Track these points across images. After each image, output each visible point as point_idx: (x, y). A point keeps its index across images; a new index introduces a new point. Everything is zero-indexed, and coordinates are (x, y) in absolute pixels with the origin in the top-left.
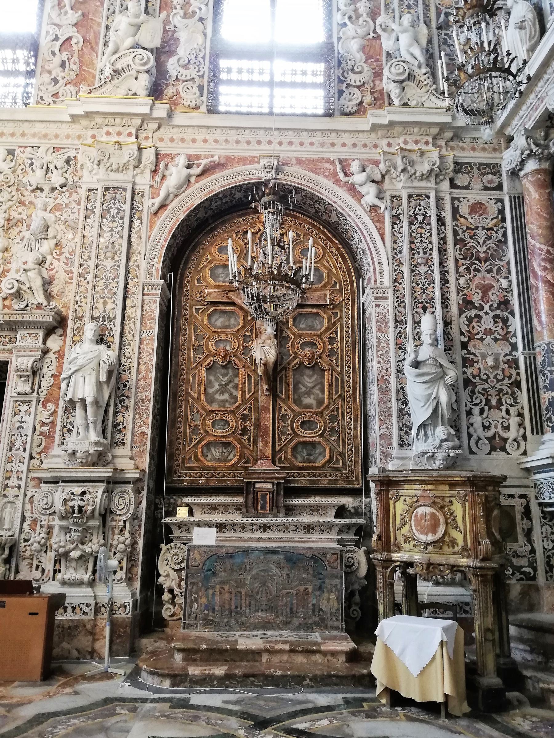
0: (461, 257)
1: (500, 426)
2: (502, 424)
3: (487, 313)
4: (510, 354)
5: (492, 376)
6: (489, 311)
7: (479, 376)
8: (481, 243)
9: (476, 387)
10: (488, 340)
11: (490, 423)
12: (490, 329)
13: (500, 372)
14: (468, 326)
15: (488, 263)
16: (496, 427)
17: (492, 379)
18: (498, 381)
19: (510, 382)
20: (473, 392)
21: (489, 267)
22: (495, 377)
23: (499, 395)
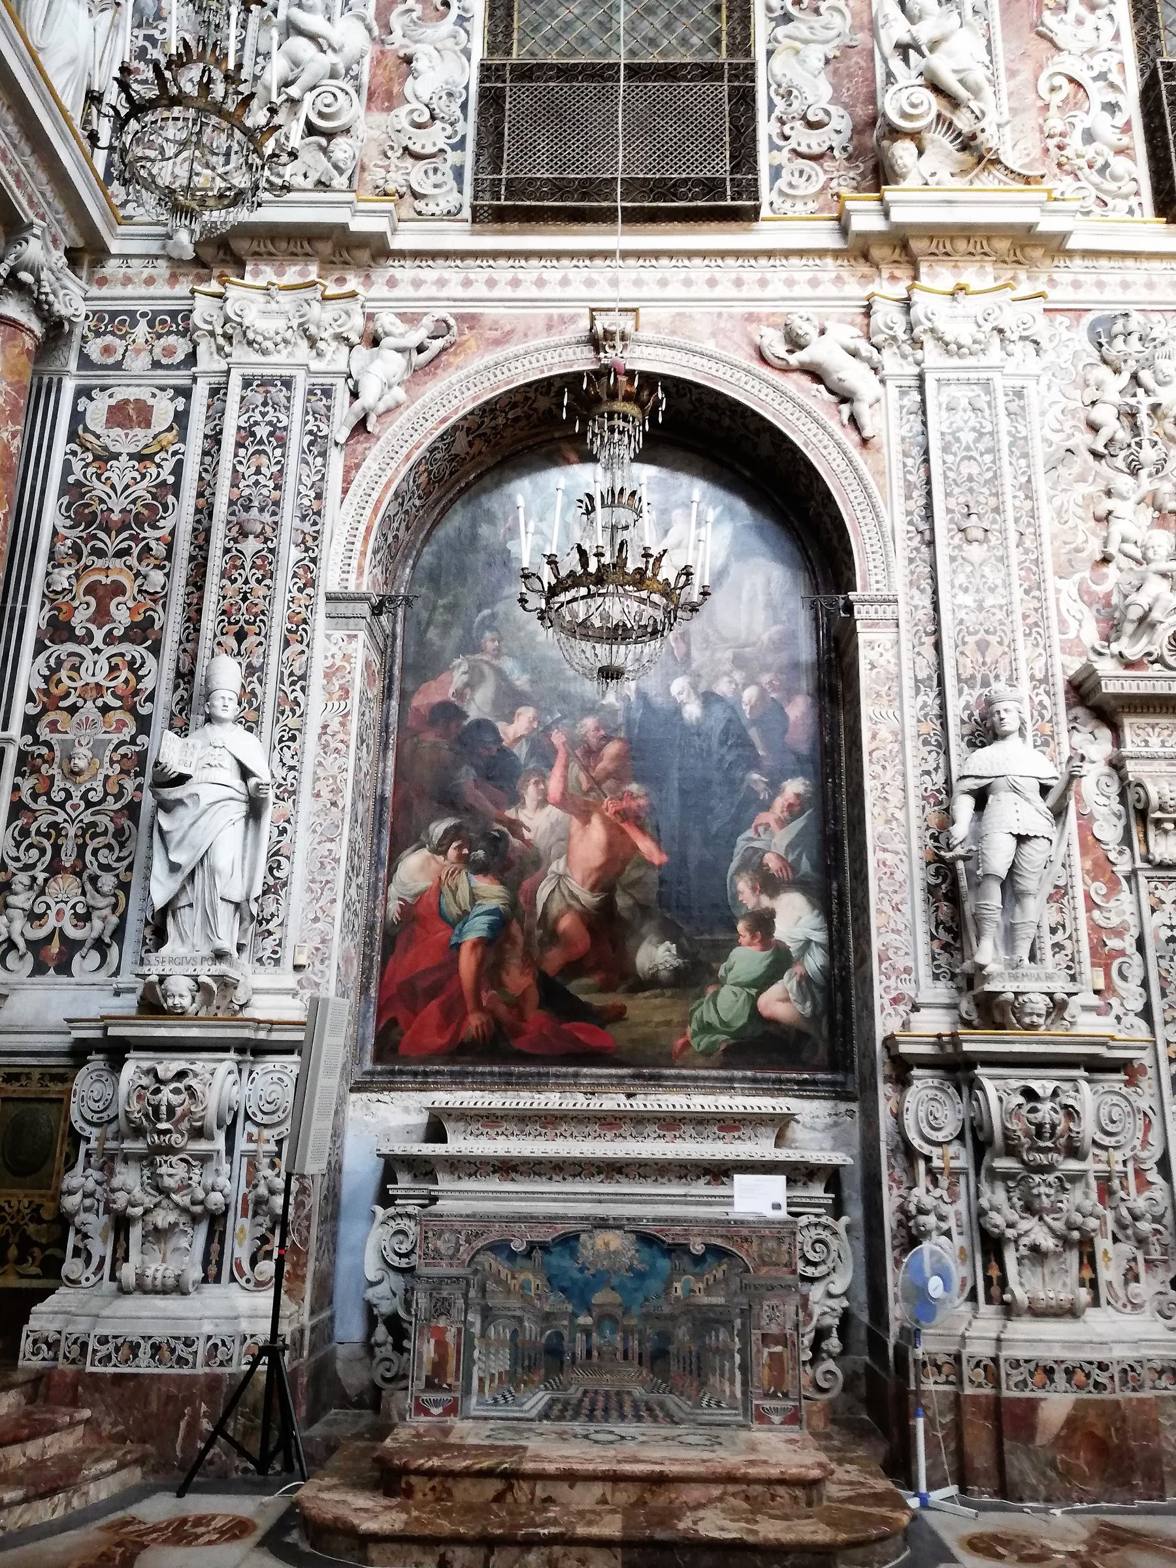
0: (69, 523)
1: (68, 913)
2: (73, 907)
3: (97, 651)
4: (133, 741)
5: (77, 794)
6: (101, 646)
7: (48, 794)
8: (119, 490)
9: (36, 819)
10: (89, 710)
11: (48, 907)
12: (97, 684)
13: (98, 784)
14: (47, 679)
15: (125, 534)
16: (60, 913)
17: (76, 800)
18: (89, 804)
19: (118, 806)
20: (24, 832)
21: (124, 545)
22: (84, 797)
23: (83, 836)
